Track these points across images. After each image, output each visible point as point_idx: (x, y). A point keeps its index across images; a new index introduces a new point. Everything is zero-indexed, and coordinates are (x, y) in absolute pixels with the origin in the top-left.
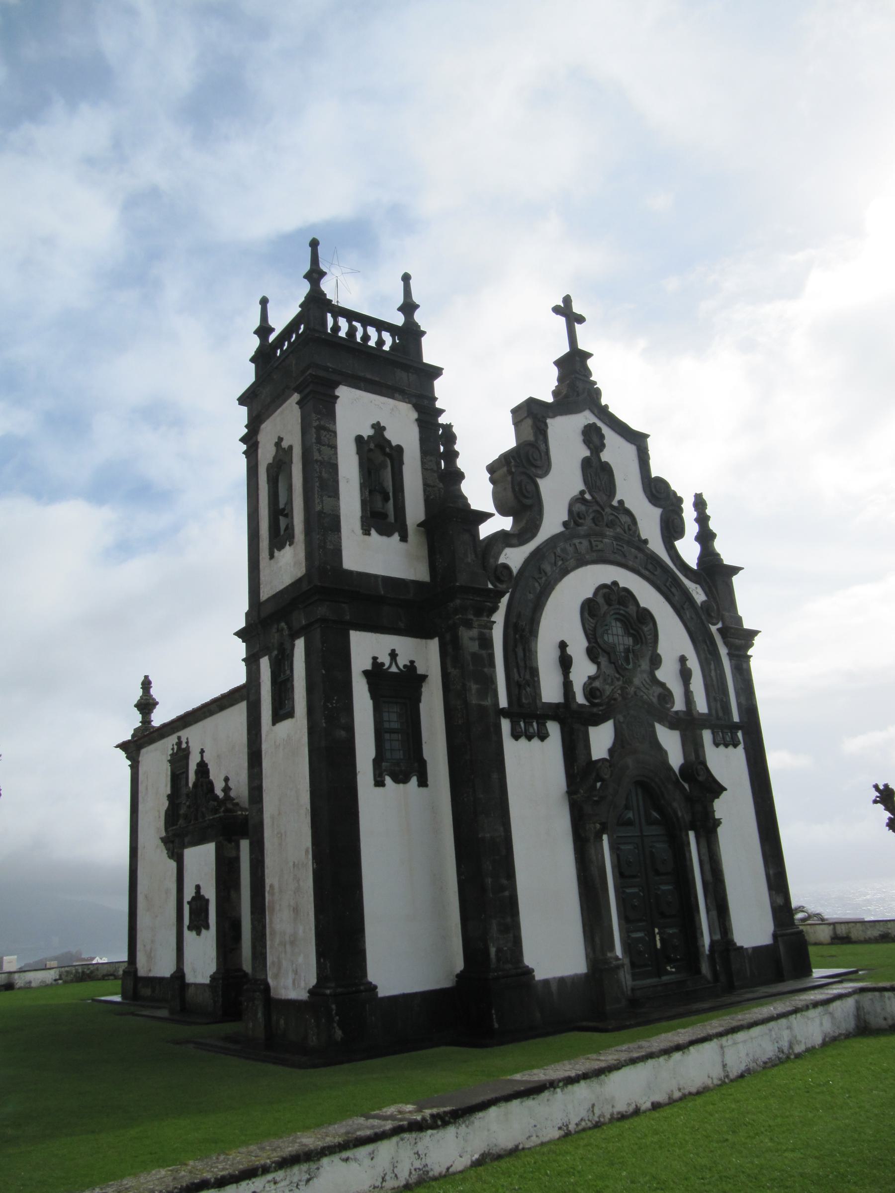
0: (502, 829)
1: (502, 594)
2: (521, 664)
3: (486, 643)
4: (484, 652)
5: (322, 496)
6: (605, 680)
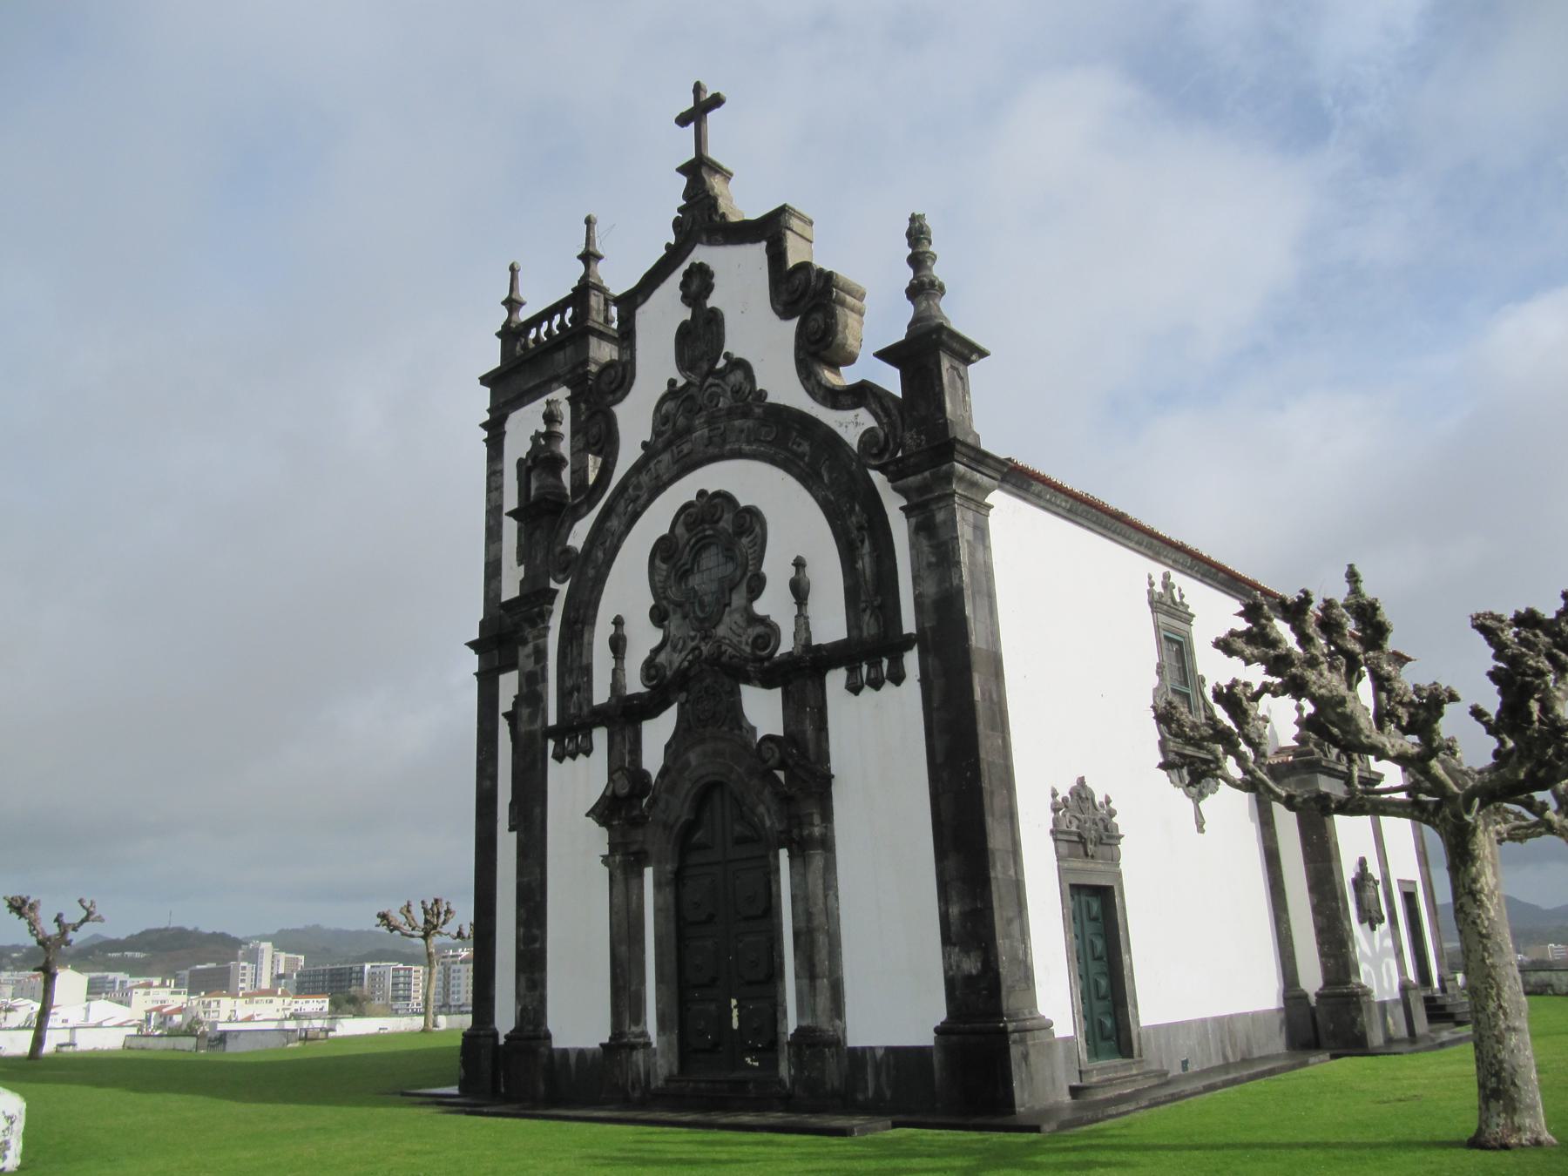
3: (540, 654)
6: (674, 648)
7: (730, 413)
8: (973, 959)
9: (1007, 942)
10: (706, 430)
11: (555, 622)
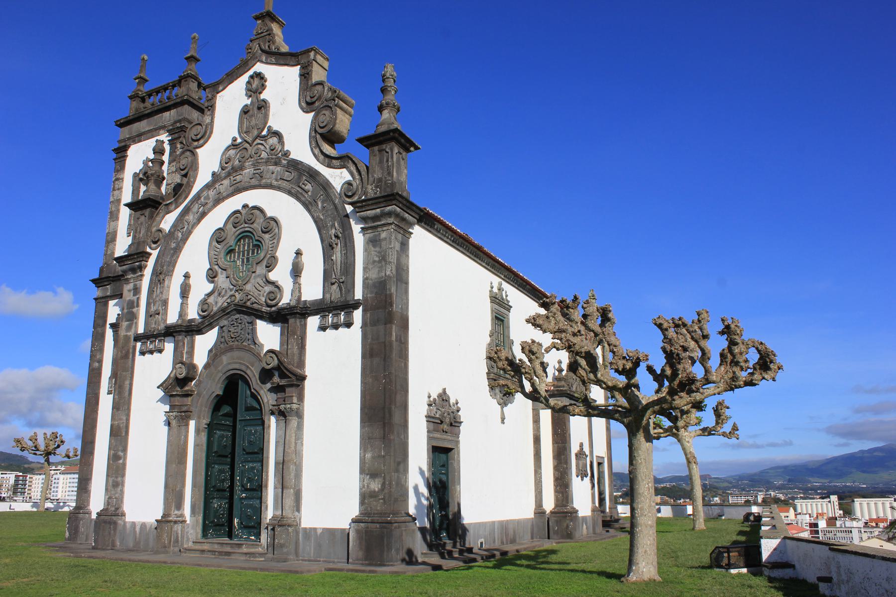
0: (125, 418)
3: (137, 291)
7: (268, 162)
8: (376, 483)
9: (396, 474)
10: (252, 169)
11: (148, 272)
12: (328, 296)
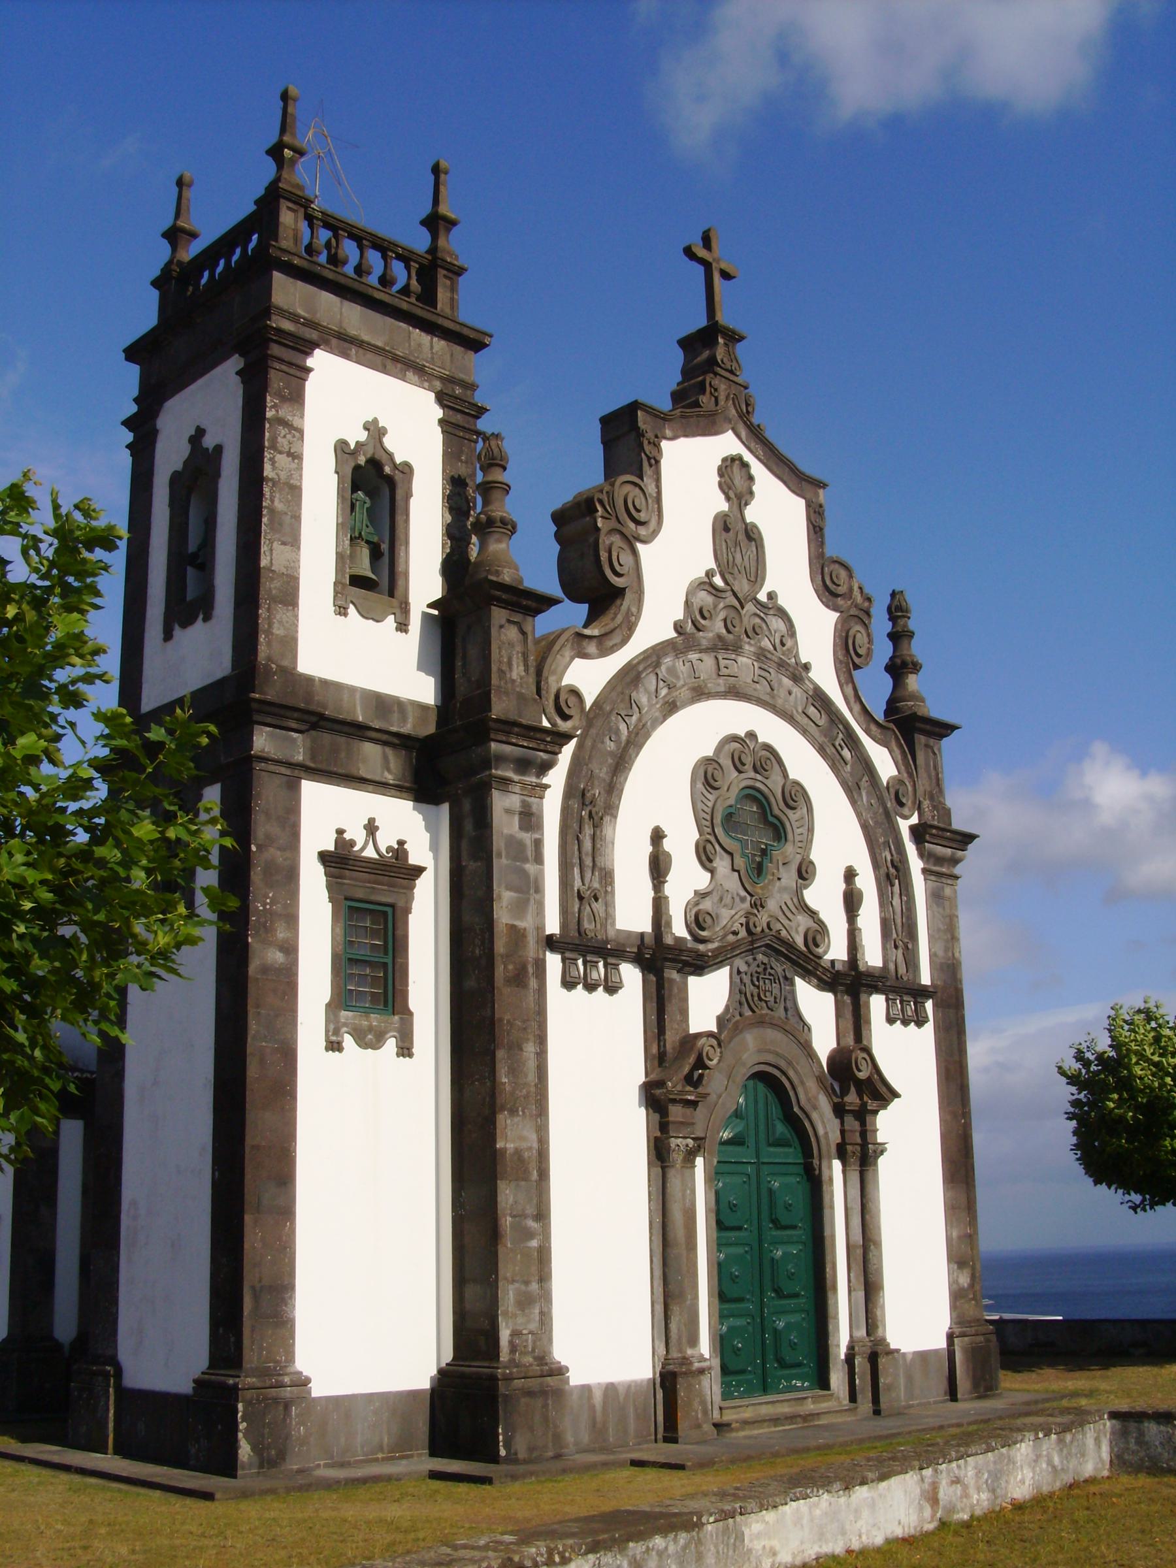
0: (534, 1137)
1: (566, 737)
2: (588, 862)
3: (530, 819)
4: (527, 837)
5: (271, 543)
12: (892, 966)
